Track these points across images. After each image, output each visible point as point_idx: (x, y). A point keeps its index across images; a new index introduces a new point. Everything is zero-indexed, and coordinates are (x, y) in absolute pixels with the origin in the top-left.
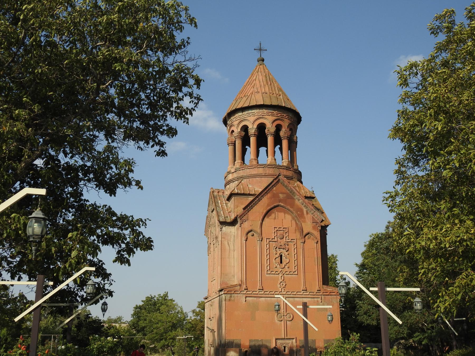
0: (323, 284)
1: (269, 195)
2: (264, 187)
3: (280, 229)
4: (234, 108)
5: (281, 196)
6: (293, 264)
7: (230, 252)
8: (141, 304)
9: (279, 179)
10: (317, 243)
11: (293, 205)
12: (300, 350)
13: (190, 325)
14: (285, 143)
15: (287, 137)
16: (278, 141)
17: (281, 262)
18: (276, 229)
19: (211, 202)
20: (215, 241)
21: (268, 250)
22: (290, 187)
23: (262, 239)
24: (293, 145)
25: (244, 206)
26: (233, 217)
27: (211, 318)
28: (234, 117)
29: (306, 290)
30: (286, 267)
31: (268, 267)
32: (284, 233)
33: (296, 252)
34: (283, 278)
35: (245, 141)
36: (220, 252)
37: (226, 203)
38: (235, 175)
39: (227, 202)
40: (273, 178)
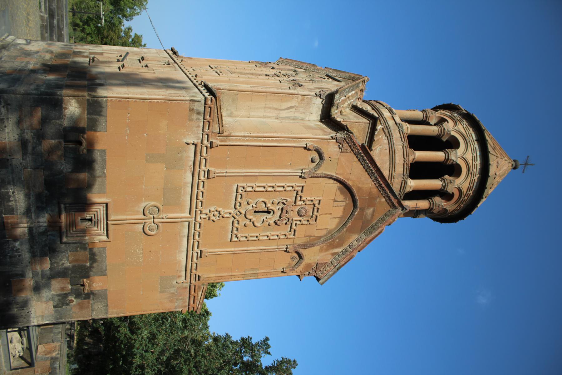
1: (375, 190)
3: (316, 210)
6: (252, 233)
7: (276, 109)
9: (396, 208)
11: (351, 231)
12: (85, 249)
13: (117, 23)
15: (432, 208)
17: (255, 212)
18: (316, 203)
19: (344, 75)
22: (381, 227)
23: (304, 178)
27: (144, 63)
29: (201, 257)
30: (247, 222)
31: (250, 189)
34: (228, 215)
36: (276, 90)
38: (391, 123)
39: (350, 106)
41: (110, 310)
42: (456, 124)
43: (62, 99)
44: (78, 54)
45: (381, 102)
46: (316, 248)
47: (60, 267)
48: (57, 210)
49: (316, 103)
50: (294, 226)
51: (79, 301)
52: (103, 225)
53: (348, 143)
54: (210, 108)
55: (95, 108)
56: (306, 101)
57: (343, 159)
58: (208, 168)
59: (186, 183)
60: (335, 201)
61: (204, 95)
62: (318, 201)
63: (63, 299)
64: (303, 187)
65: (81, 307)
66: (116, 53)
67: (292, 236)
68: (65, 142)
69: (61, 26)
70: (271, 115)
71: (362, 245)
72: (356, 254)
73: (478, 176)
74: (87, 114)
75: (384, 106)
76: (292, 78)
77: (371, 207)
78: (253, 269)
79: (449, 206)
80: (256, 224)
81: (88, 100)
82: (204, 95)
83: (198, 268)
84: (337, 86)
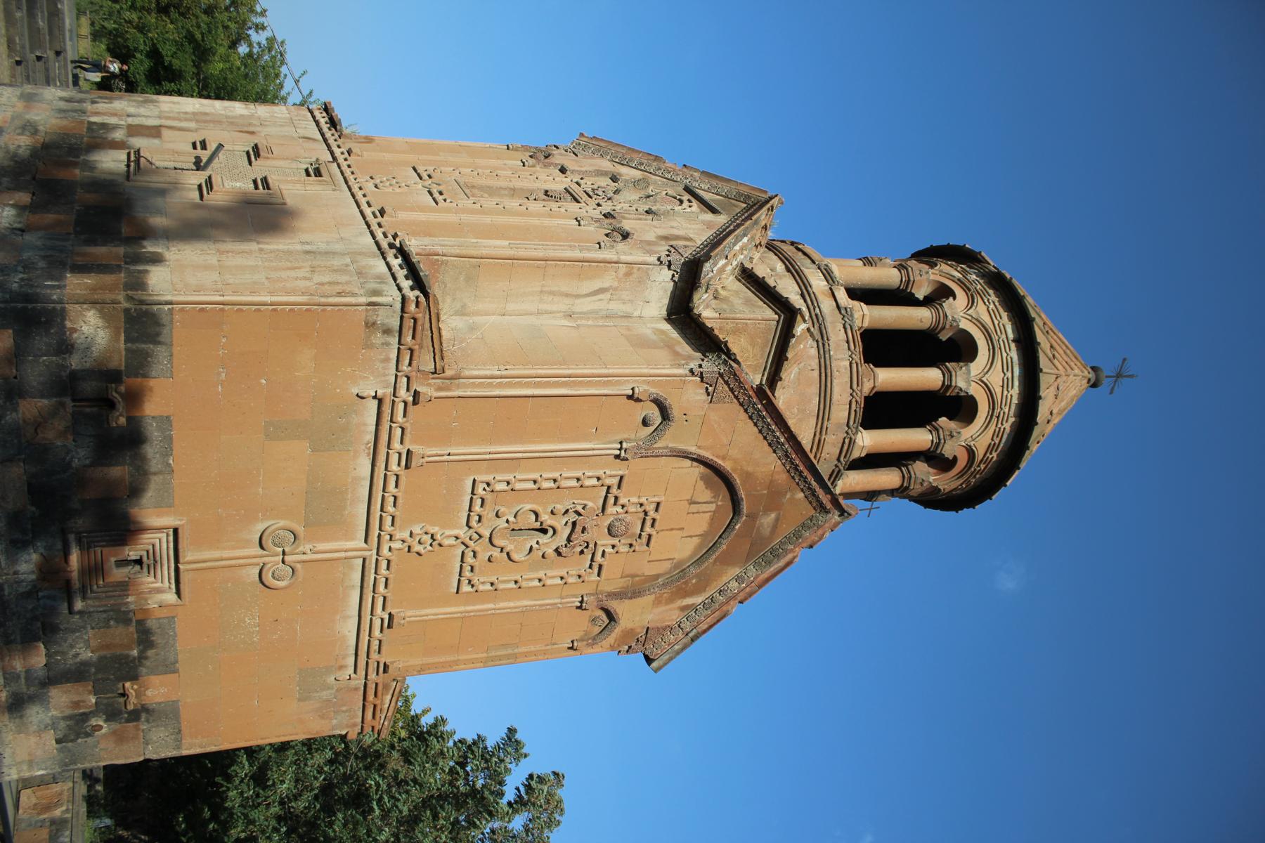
1: (782, 477)
3: (649, 523)
4: (1033, 314)
5: (768, 520)
7: (567, 295)
9: (827, 512)
11: (726, 560)
12: (127, 622)
15: (907, 488)
19: (726, 188)
22: (792, 551)
29: (390, 626)
30: (496, 553)
31: (503, 486)
32: (632, 536)
38: (827, 305)
41: (186, 741)
42: (971, 302)
43: (63, 310)
45: (808, 249)
46: (648, 599)
47: (71, 662)
48: (59, 545)
49: (660, 279)
50: (598, 558)
51: (115, 726)
52: (167, 570)
53: (726, 383)
54: (415, 320)
56: (635, 276)
57: (713, 416)
58: (408, 445)
59: (356, 480)
60: (692, 502)
61: (400, 289)
62: (654, 505)
63: (77, 723)
64: (622, 477)
65: (120, 738)
66: (192, 125)
67: (594, 577)
68: (74, 401)
70: (554, 308)
71: (748, 590)
72: (735, 608)
73: (1012, 420)
74: (126, 342)
75: (813, 262)
76: (607, 207)
77: (771, 510)
78: (504, 646)
79: (945, 482)
80: (515, 556)
81: (127, 311)
82: (400, 289)
83: (383, 648)
84: (709, 225)
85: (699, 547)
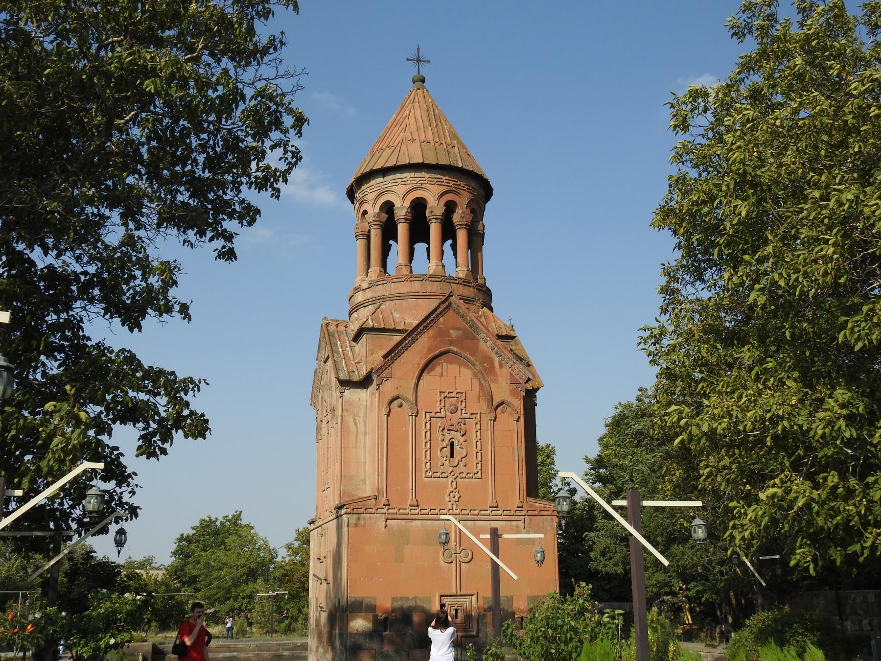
0: (528, 495)
1: (431, 332)
2: (423, 317)
3: (451, 395)
4: (368, 170)
6: (473, 460)
7: (357, 436)
8: (191, 532)
10: (518, 421)
11: (474, 351)
12: (484, 616)
13: (282, 571)
14: (462, 236)
15: (466, 225)
16: (448, 232)
17: (452, 456)
19: (323, 344)
20: (329, 416)
21: (428, 434)
23: (417, 412)
24: (476, 239)
25: (384, 352)
26: (364, 372)
27: (322, 558)
28: (367, 186)
30: (461, 464)
32: (457, 401)
33: (479, 437)
34: (454, 484)
35: (389, 232)
36: (339, 438)
37: (351, 347)
38: (369, 294)
39: (354, 344)
40: (439, 301)
44: (318, 621)
50: (467, 416)
55: (356, 607)
69: (292, 646)
70: (363, 441)
73: (424, 174)
78: (513, 453)
85: (466, 366)
